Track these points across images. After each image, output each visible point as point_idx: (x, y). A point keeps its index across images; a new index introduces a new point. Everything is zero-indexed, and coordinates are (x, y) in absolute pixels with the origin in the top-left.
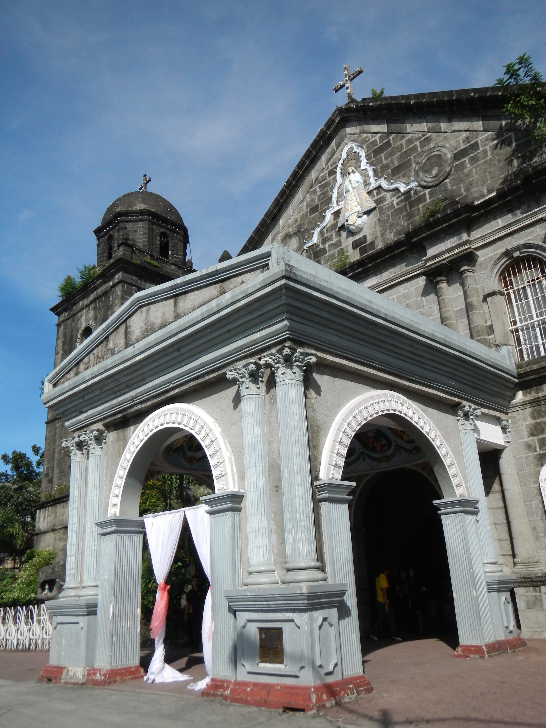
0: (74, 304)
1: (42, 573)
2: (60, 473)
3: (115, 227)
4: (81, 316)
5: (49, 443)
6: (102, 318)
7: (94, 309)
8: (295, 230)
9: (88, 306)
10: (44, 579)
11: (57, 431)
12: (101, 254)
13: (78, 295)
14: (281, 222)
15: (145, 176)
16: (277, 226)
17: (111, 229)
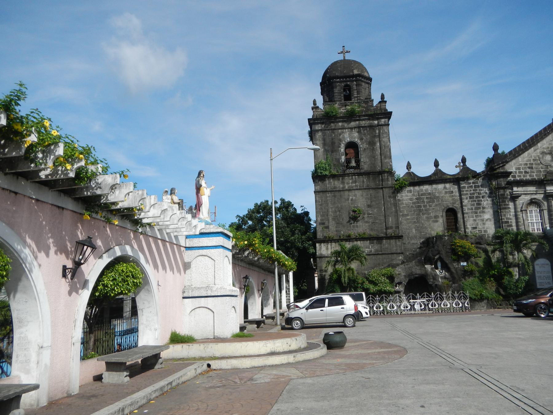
0: (333, 122)
1: (397, 279)
2: (337, 224)
3: (353, 81)
4: (343, 132)
5: (321, 205)
6: (368, 140)
7: (358, 132)
8: (548, 152)
9: (351, 128)
10: (399, 281)
11: (328, 198)
12: (338, 93)
13: (340, 119)
14: (539, 145)
15: (343, 47)
16: (536, 146)
17: (349, 81)
